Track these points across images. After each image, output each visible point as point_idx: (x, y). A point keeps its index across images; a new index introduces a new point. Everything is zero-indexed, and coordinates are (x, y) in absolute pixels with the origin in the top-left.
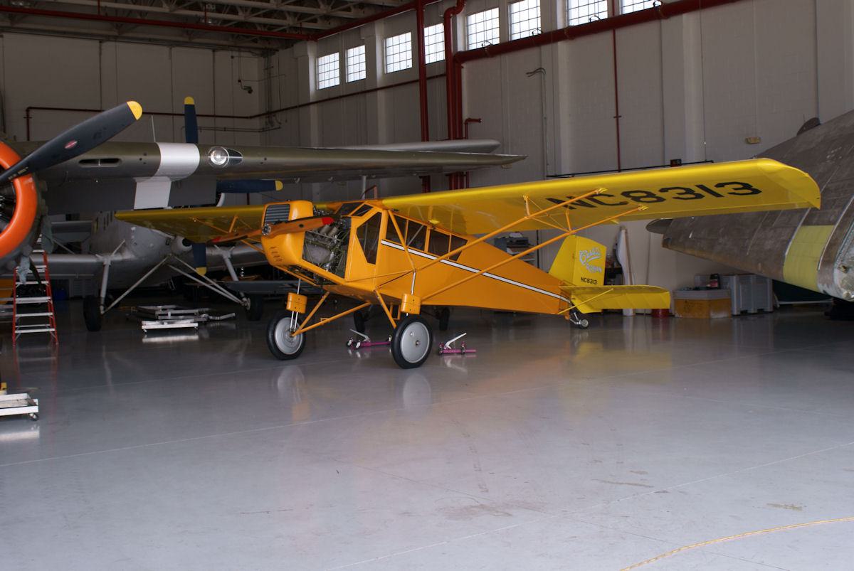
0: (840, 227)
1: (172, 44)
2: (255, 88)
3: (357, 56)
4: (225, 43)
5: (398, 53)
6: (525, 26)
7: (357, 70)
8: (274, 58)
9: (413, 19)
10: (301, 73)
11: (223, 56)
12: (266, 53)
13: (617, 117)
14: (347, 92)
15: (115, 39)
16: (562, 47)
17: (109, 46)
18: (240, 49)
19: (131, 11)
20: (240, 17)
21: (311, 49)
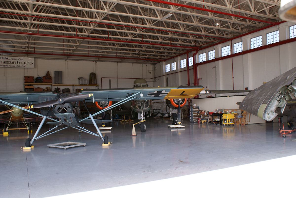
0: (268, 105)
1: (133, 63)
2: (152, 72)
3: (174, 64)
4: (145, 62)
5: (183, 63)
6: (212, 57)
7: (174, 68)
8: (156, 65)
9: (186, 56)
10: (162, 69)
11: (144, 65)
12: (154, 64)
13: (233, 78)
14: (173, 73)
15: (121, 62)
16: (220, 62)
17: (119, 64)
18: (148, 63)
19: (124, 56)
20: (148, 56)
21: (164, 63)
